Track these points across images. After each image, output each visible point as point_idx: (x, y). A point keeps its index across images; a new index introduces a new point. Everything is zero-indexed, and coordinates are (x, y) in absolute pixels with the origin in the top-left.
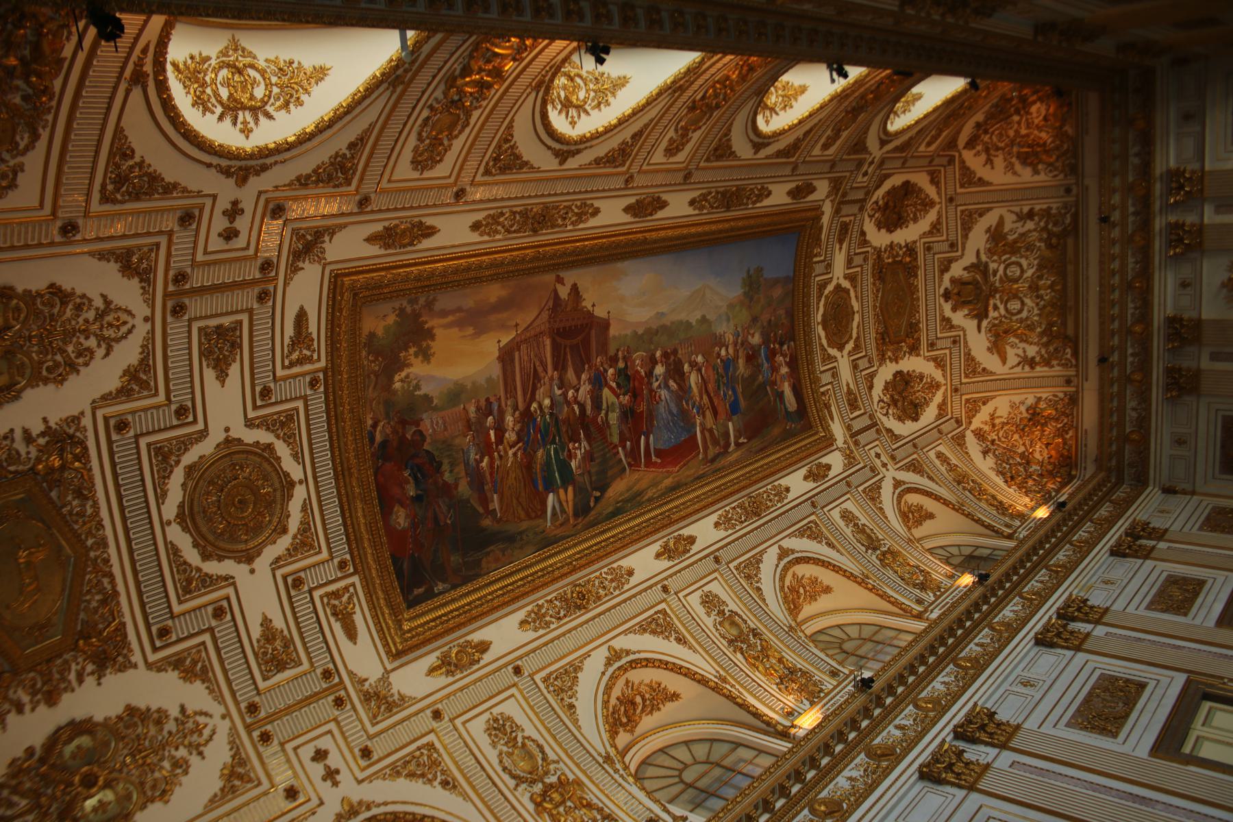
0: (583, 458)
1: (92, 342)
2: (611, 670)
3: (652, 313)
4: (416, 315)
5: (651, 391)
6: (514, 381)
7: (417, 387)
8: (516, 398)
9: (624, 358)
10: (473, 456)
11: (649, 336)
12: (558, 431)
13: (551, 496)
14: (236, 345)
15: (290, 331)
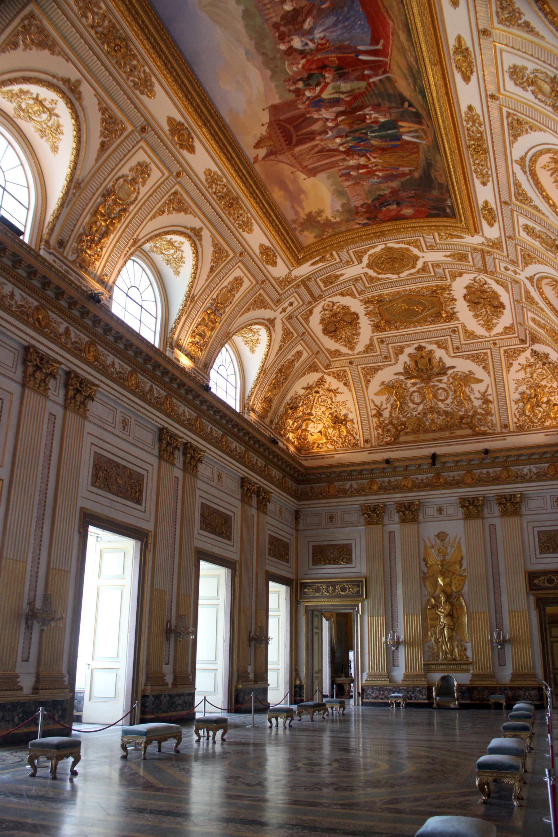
0: (378, 112)
1: (335, 307)
2: (528, 174)
3: (249, 65)
4: (302, 224)
5: (318, 50)
6: (327, 164)
7: (338, 211)
8: (338, 161)
9: (295, 83)
10: (375, 180)
11: (270, 62)
12: (357, 131)
13: (406, 138)
14: (330, 276)
15: (321, 264)
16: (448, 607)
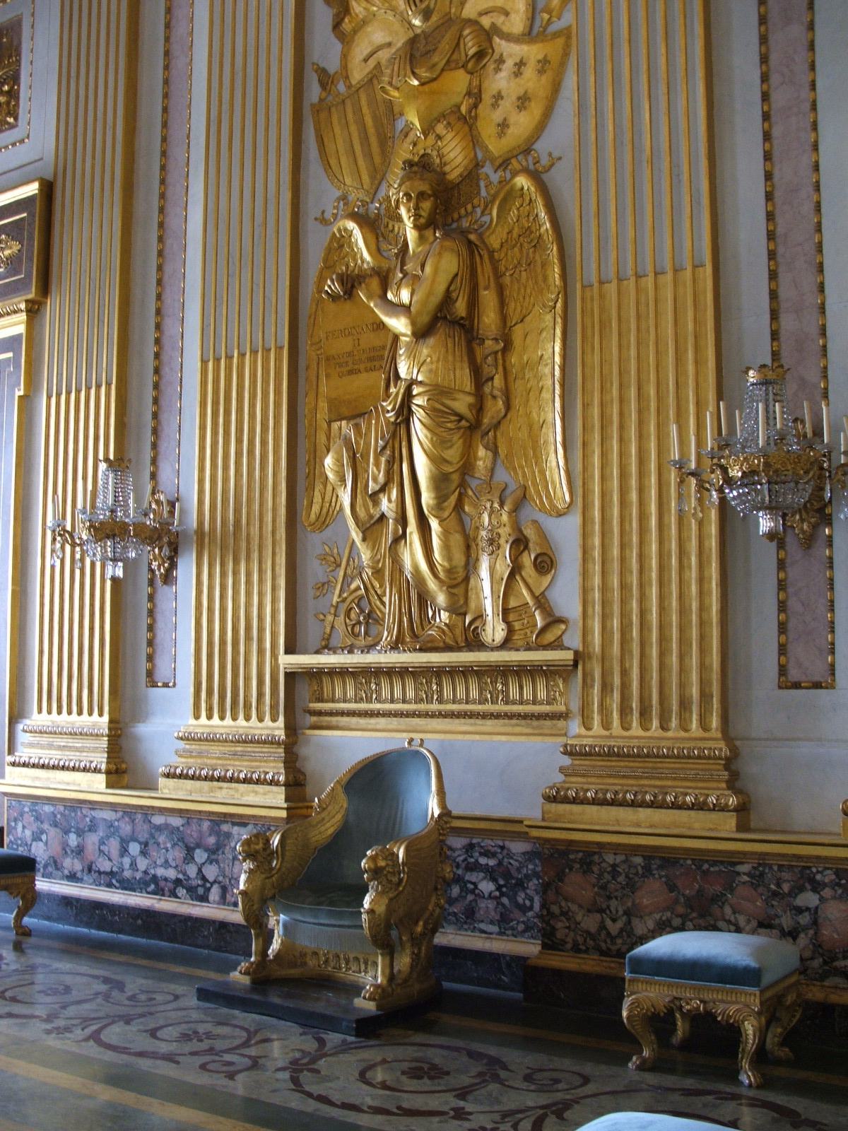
16: (441, 267)
